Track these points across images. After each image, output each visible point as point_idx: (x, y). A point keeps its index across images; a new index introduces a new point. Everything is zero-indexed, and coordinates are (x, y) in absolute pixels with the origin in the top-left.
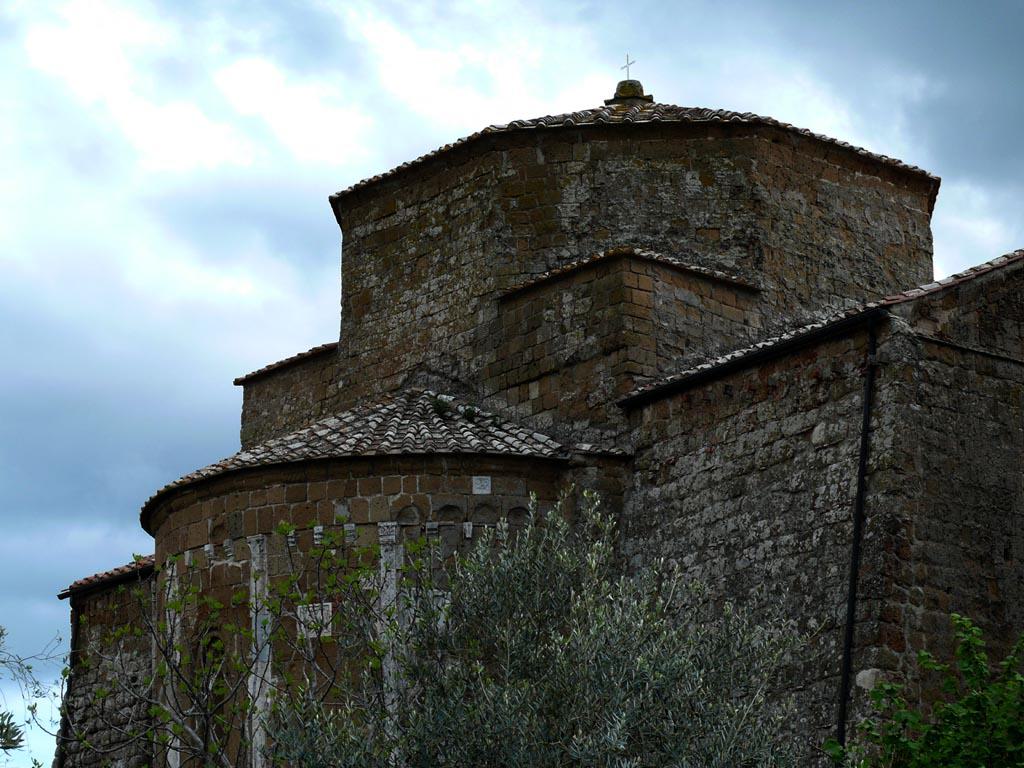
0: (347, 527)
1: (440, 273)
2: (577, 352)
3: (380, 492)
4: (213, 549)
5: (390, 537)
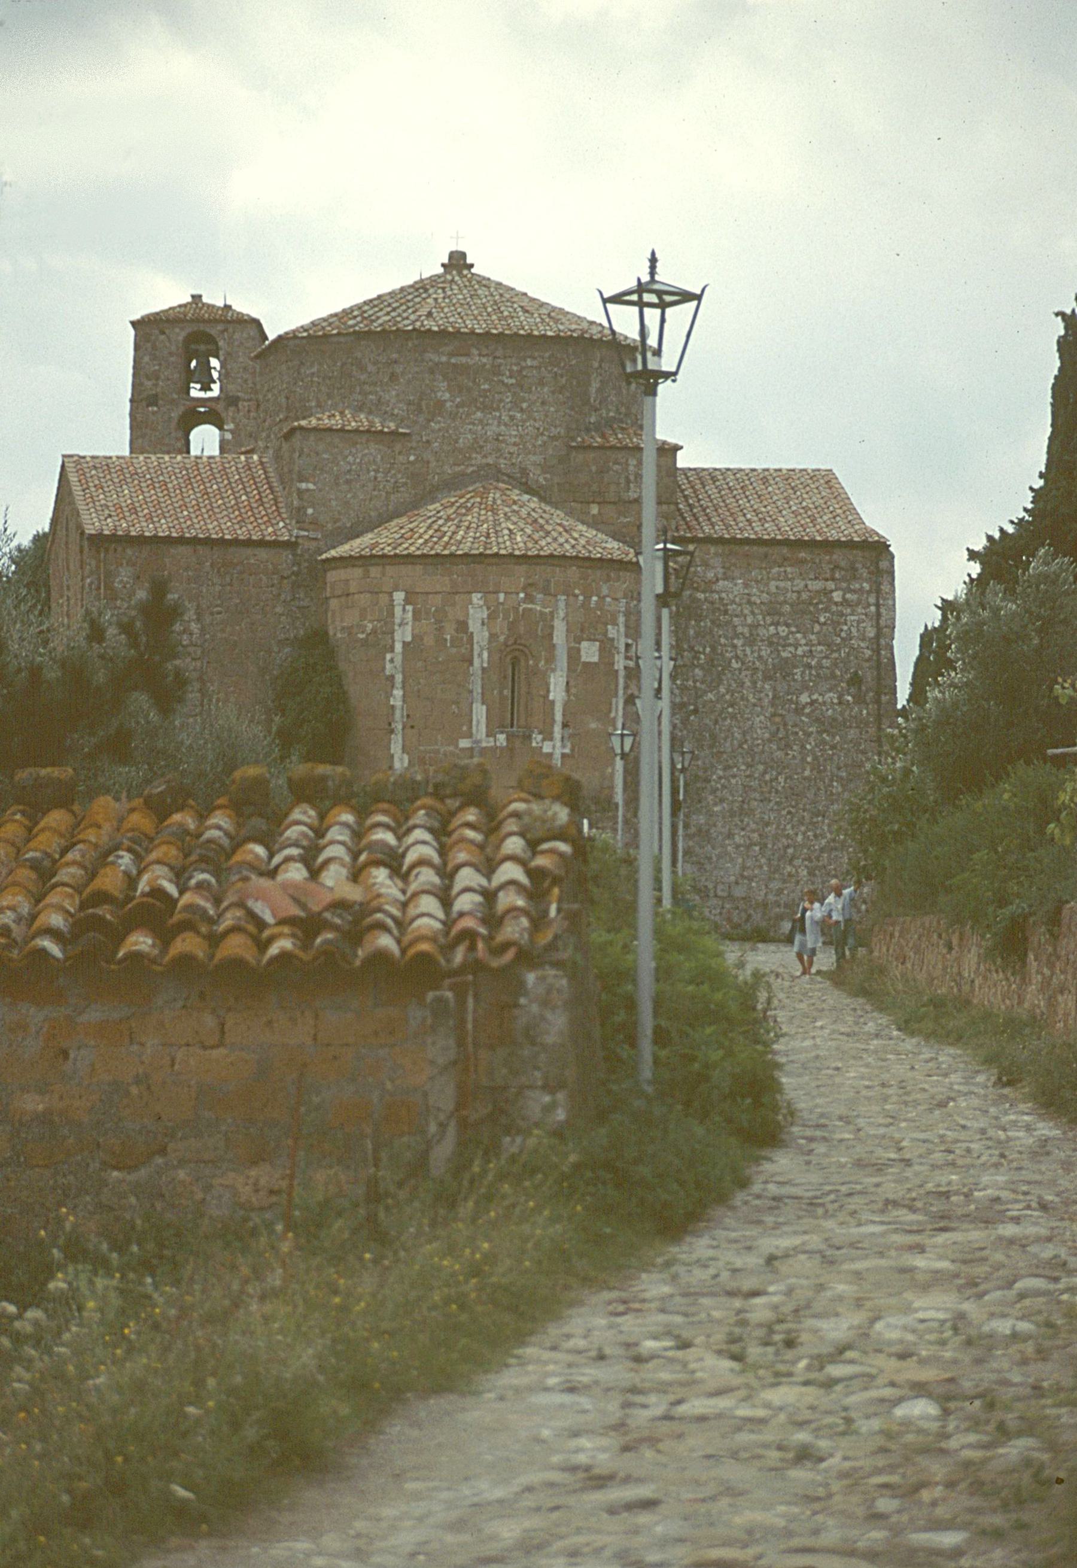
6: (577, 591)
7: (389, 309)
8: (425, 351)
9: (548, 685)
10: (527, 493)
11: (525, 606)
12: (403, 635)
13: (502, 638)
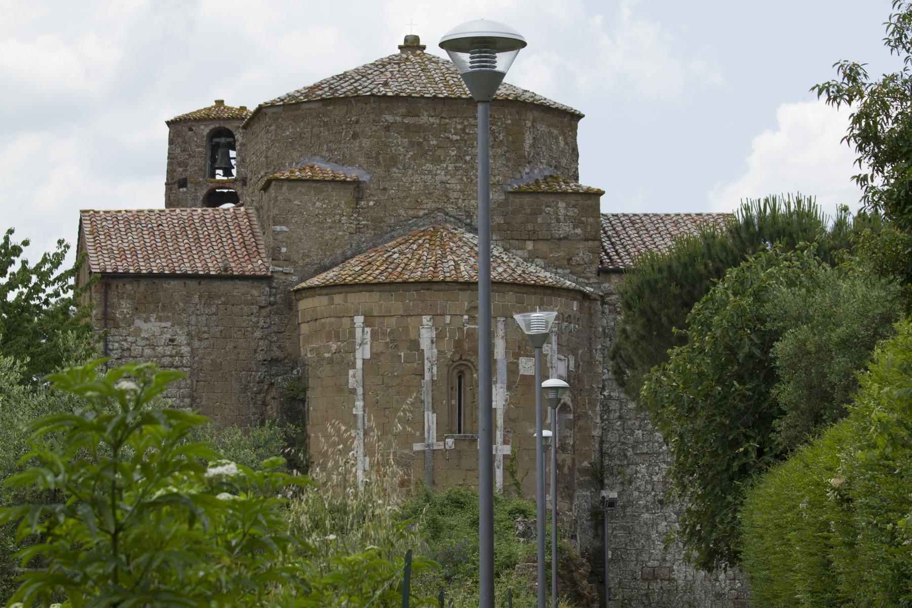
1: (456, 161)
7: (352, 81)
8: (381, 113)
10: (470, 232)
11: (468, 326)
12: (363, 353)
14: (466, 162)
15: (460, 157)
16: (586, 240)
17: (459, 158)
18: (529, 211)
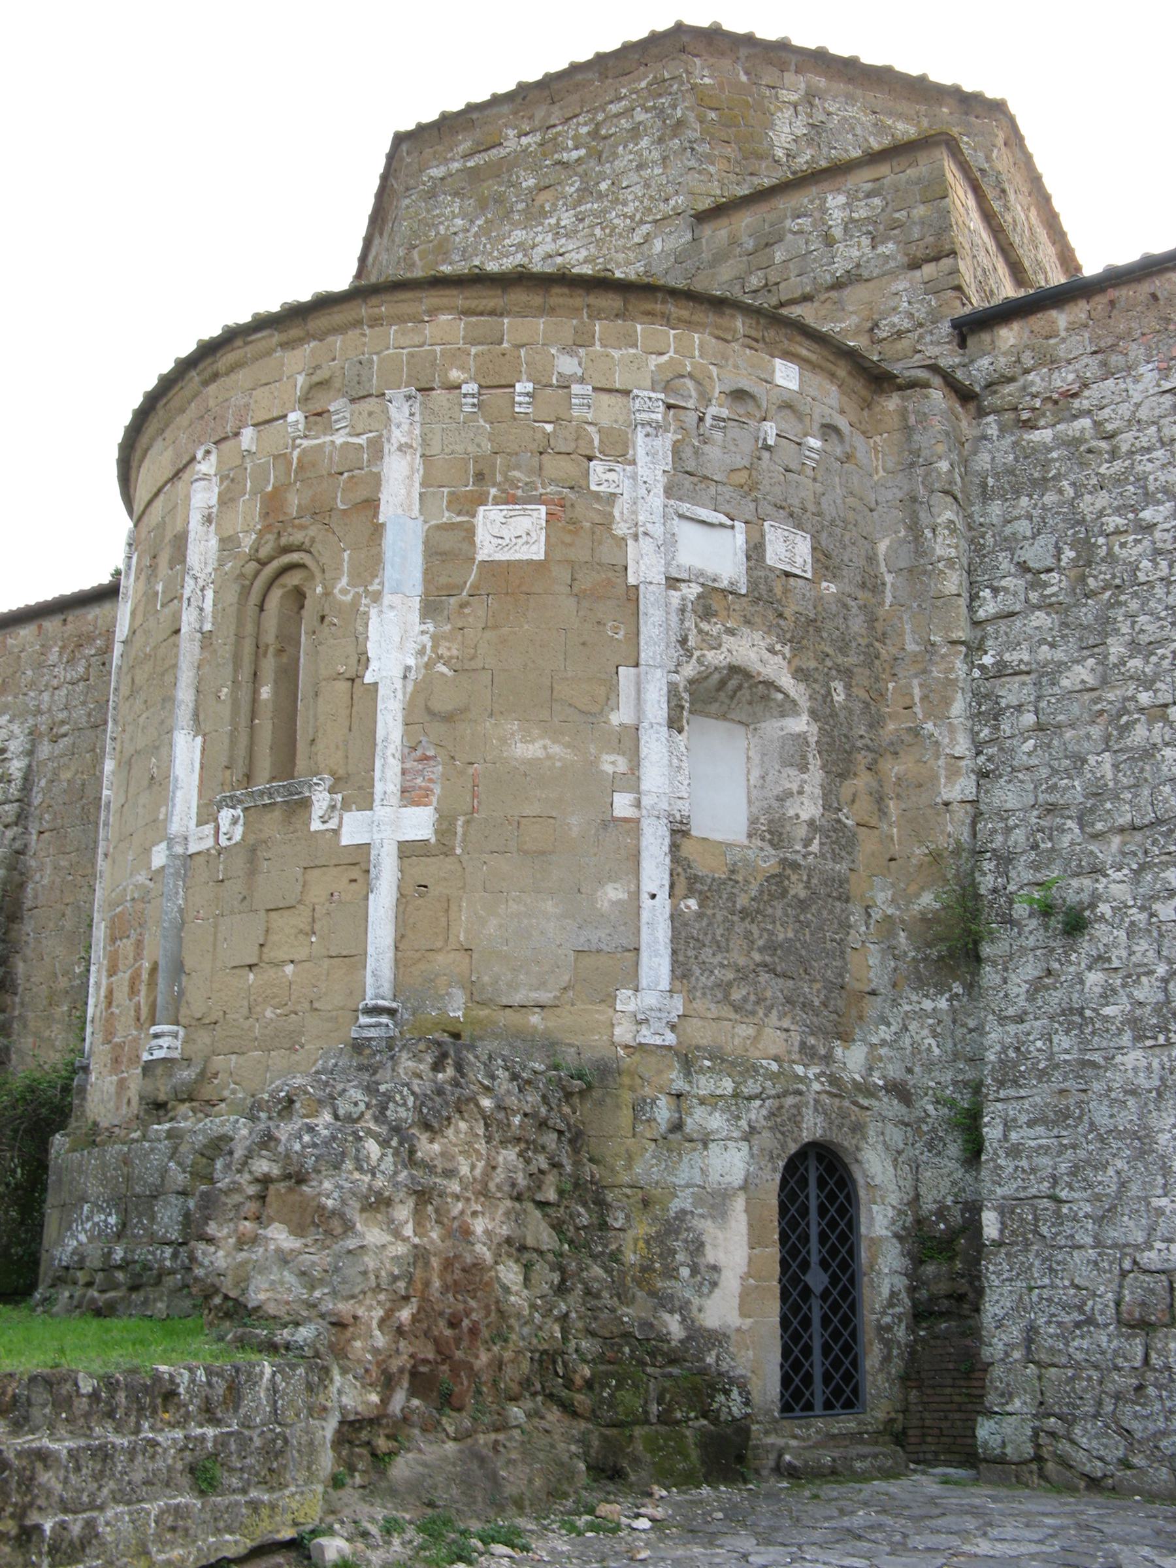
0: (576, 388)
2: (858, 266)
3: (635, 346)
4: (302, 420)
5: (653, 416)
6: (455, 375)
9: (359, 641)
13: (247, 542)
14: (601, 196)
15: (585, 189)
16: (915, 265)
17: (586, 192)
18: (750, 244)
